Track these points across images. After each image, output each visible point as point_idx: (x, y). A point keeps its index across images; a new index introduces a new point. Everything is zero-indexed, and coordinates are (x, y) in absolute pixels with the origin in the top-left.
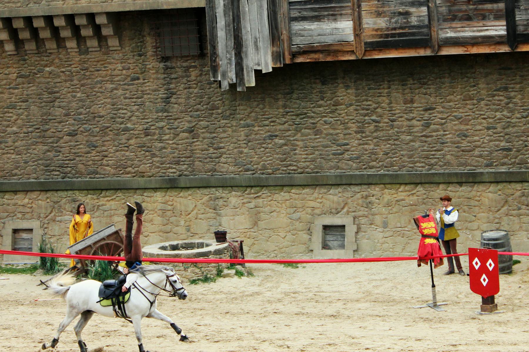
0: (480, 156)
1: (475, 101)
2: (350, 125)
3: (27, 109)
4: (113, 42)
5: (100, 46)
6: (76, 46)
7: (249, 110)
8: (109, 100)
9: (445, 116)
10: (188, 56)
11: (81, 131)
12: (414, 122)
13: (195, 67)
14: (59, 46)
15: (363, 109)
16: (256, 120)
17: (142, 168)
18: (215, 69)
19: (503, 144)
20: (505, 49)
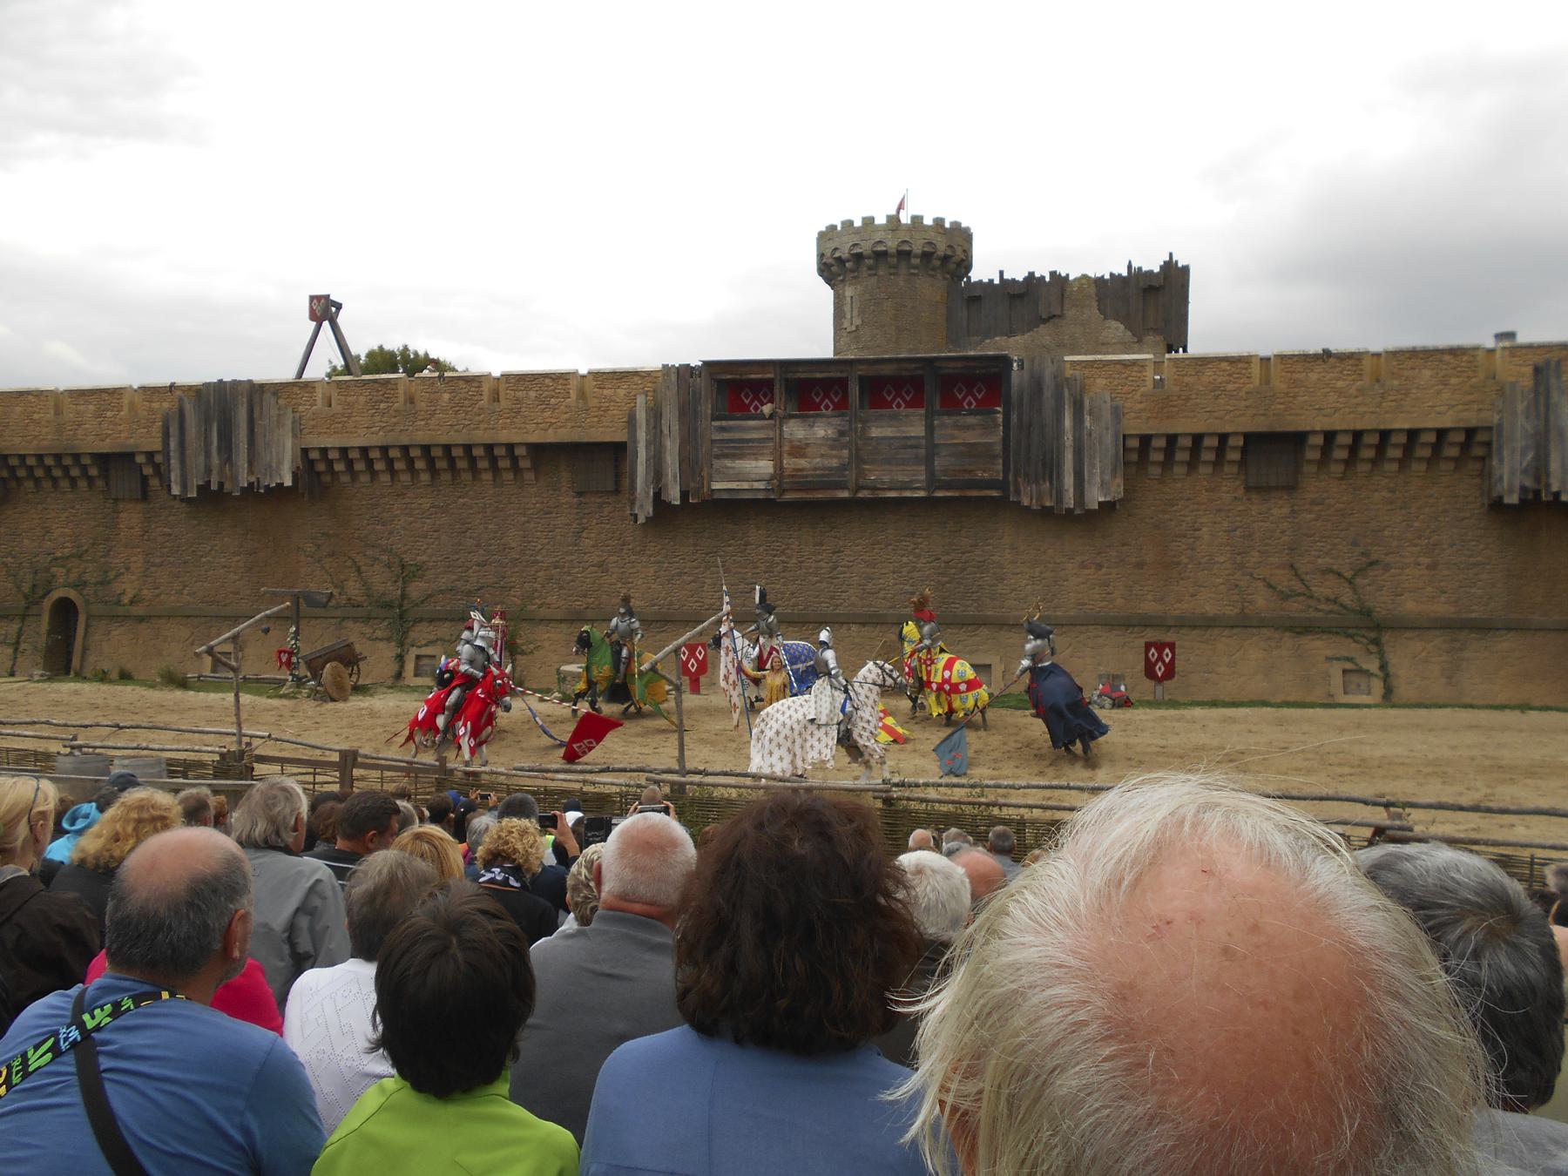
0: (884, 599)
1: (883, 546)
2: (759, 564)
3: (438, 538)
4: (529, 476)
5: (515, 479)
6: (491, 478)
7: (659, 547)
8: (520, 533)
9: (852, 559)
10: (602, 492)
11: (492, 562)
12: (822, 564)
13: (609, 503)
14: (474, 479)
15: (773, 550)
16: (666, 557)
17: (548, 600)
18: (633, 503)
19: (907, 587)
20: (922, 494)
